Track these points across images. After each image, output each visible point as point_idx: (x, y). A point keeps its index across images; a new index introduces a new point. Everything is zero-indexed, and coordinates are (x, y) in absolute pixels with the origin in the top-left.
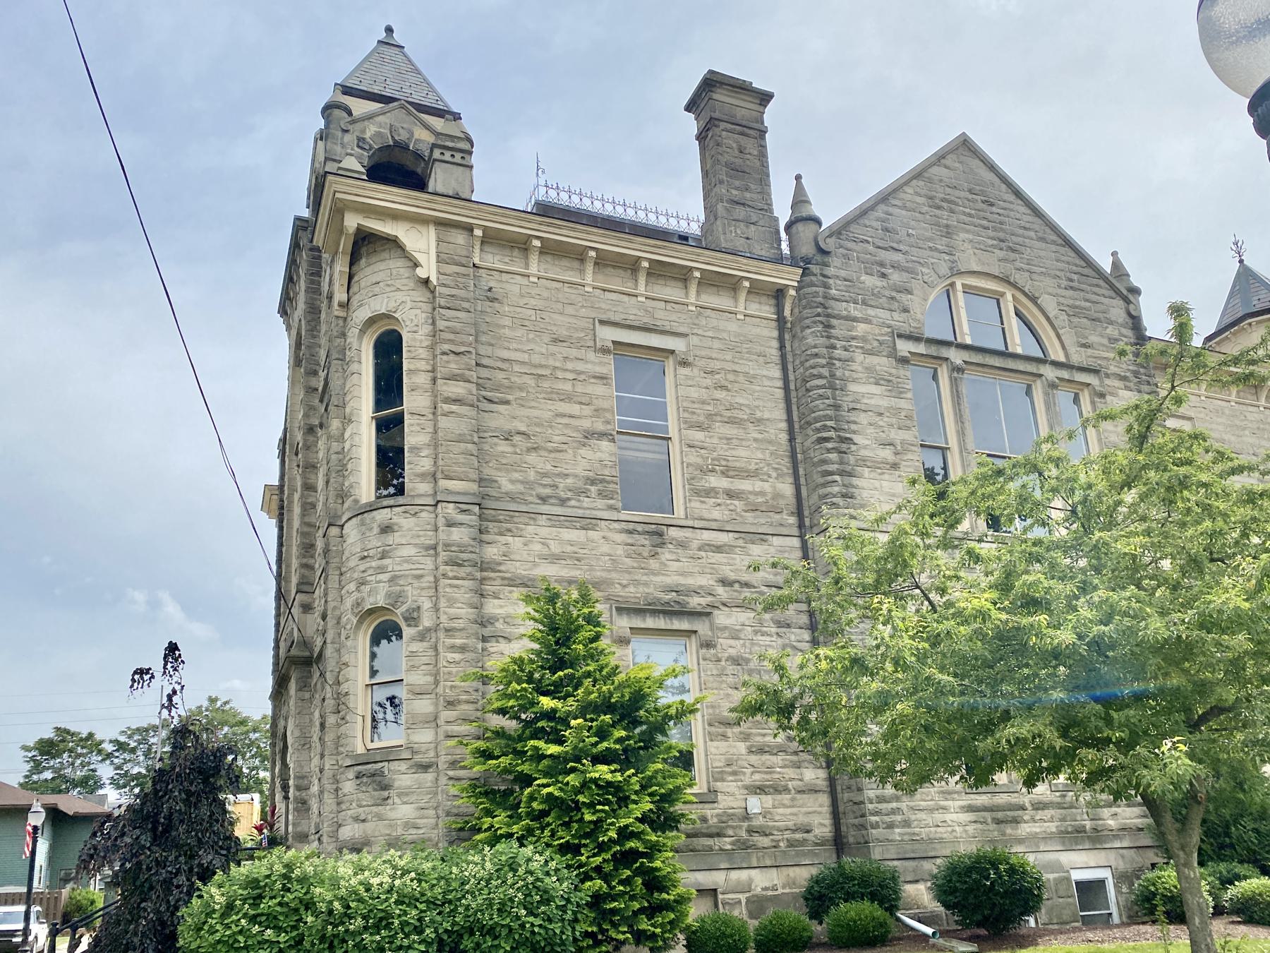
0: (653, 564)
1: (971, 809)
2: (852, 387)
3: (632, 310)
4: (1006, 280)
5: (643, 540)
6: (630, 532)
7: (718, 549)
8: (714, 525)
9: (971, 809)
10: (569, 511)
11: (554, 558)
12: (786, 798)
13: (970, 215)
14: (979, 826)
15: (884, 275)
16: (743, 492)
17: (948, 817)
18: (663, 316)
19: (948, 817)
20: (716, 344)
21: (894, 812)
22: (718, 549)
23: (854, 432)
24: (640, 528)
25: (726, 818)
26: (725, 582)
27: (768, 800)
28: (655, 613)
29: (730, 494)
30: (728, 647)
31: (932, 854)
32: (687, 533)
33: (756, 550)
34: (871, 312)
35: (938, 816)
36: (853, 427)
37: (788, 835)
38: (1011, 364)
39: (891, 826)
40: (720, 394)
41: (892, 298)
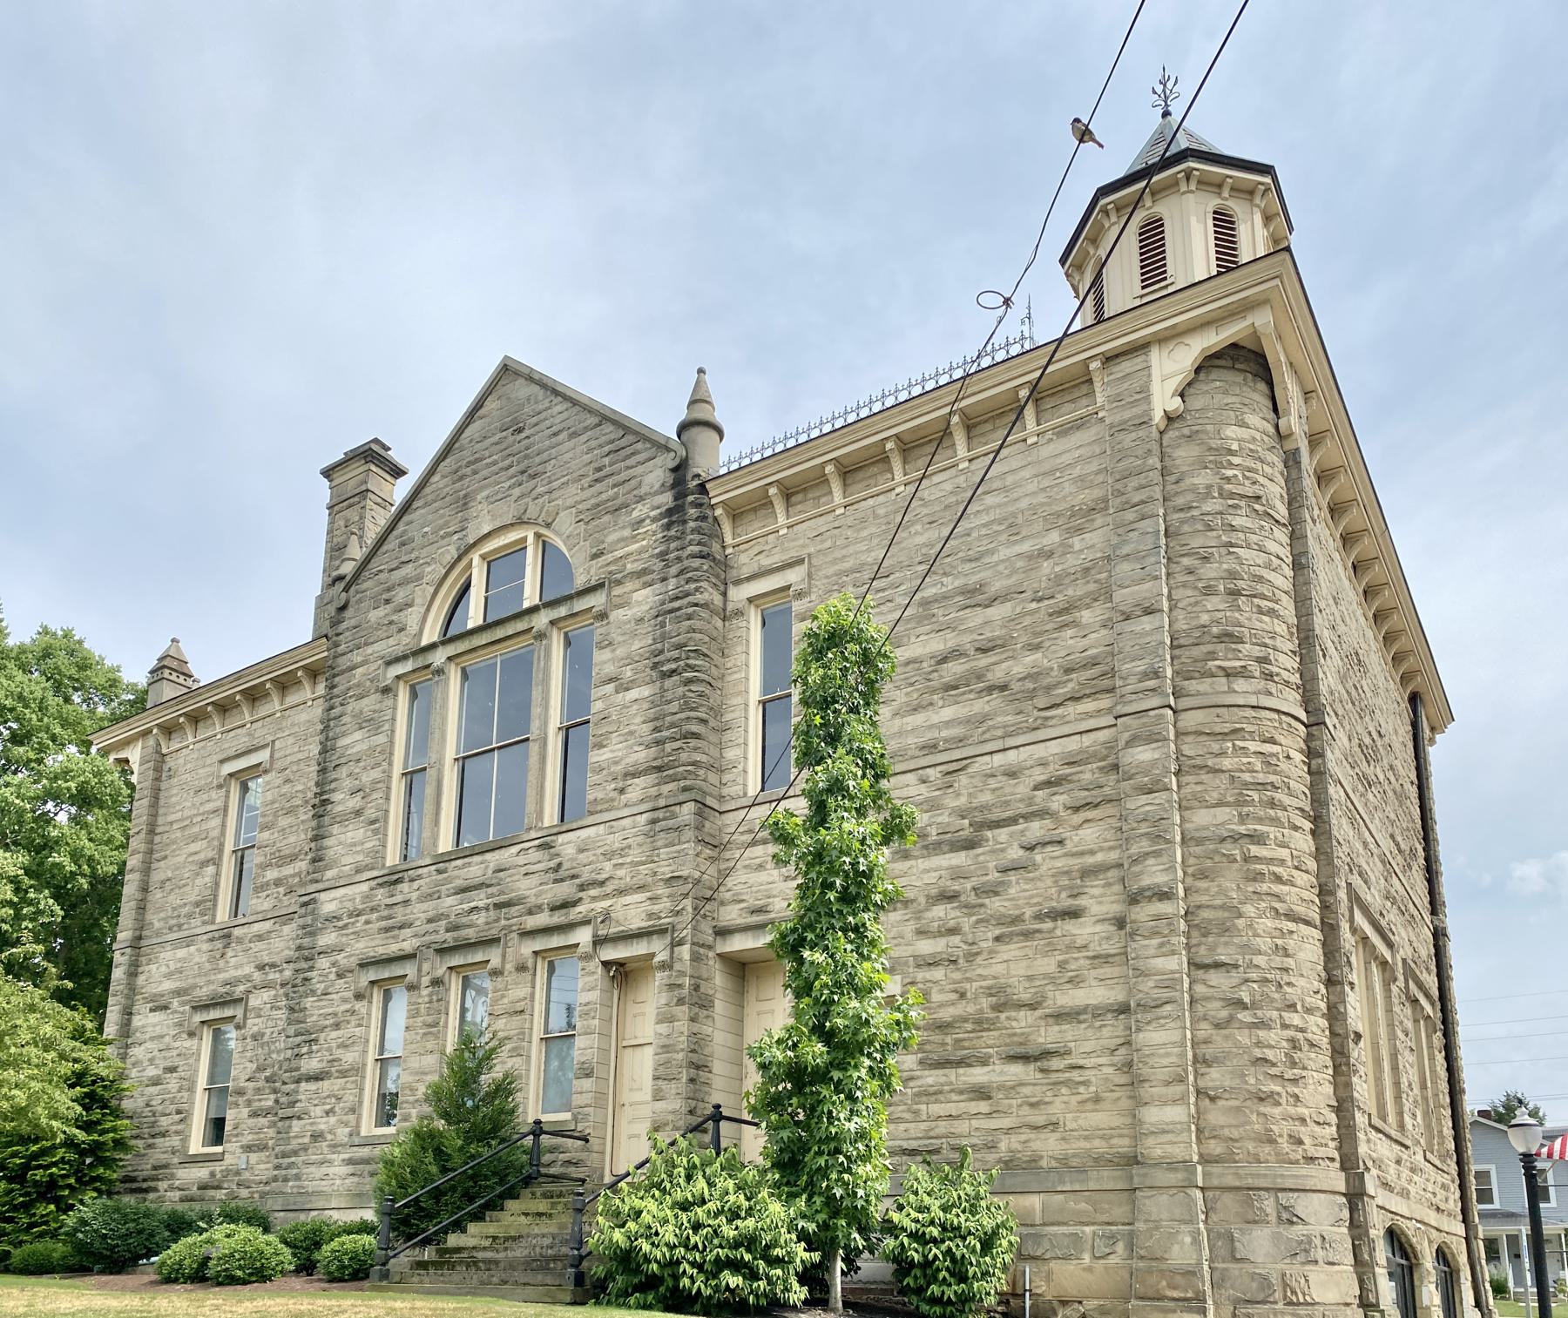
0: (221, 963)
1: (350, 1162)
2: (341, 743)
3: (240, 740)
4: (520, 522)
5: (219, 944)
6: (212, 940)
7: (260, 937)
8: (260, 917)
9: (350, 1162)
10: (186, 933)
11: (169, 976)
12: (263, 1155)
13: (494, 463)
14: (356, 1179)
15: (387, 601)
16: (286, 877)
17: (331, 1171)
18: (262, 732)
19: (331, 1171)
20: (291, 740)
21: (289, 1166)
22: (260, 937)
23: (334, 791)
24: (216, 935)
25: (227, 1173)
26: (261, 967)
27: (254, 1157)
28: (214, 1005)
29: (278, 883)
30: (254, 1025)
31: (308, 1206)
32: (245, 929)
33: (286, 929)
34: (369, 650)
35: (324, 1170)
36: (333, 785)
37: (262, 1188)
38: (500, 633)
39: (286, 1180)
40: (286, 789)
41: (391, 623)
